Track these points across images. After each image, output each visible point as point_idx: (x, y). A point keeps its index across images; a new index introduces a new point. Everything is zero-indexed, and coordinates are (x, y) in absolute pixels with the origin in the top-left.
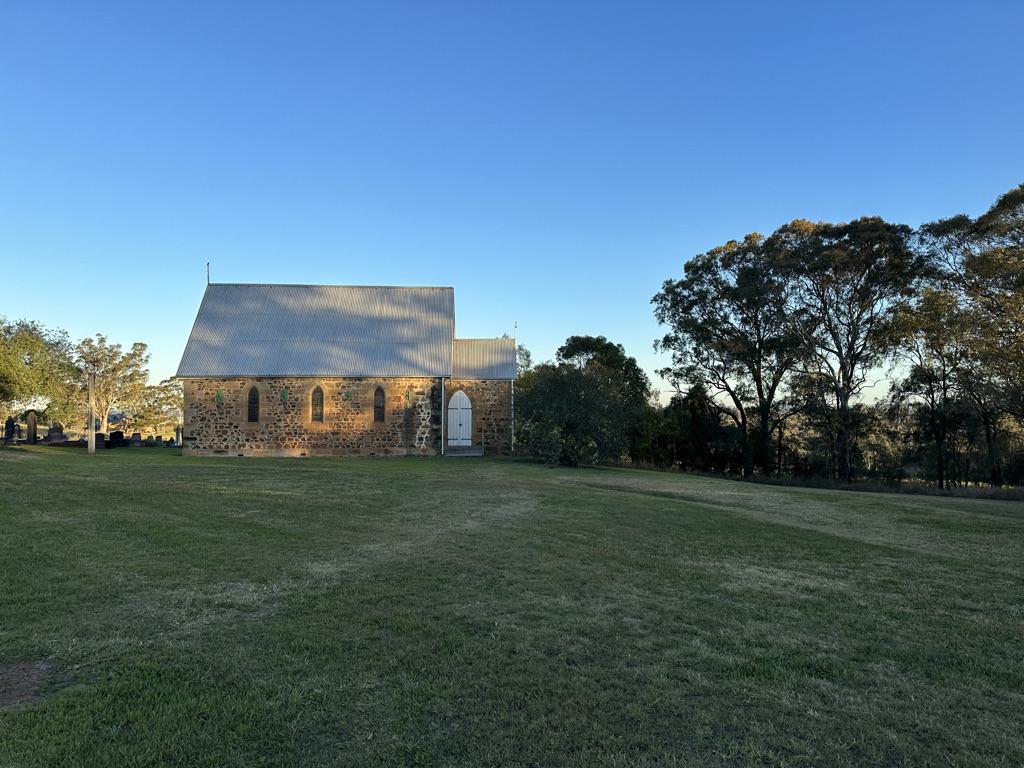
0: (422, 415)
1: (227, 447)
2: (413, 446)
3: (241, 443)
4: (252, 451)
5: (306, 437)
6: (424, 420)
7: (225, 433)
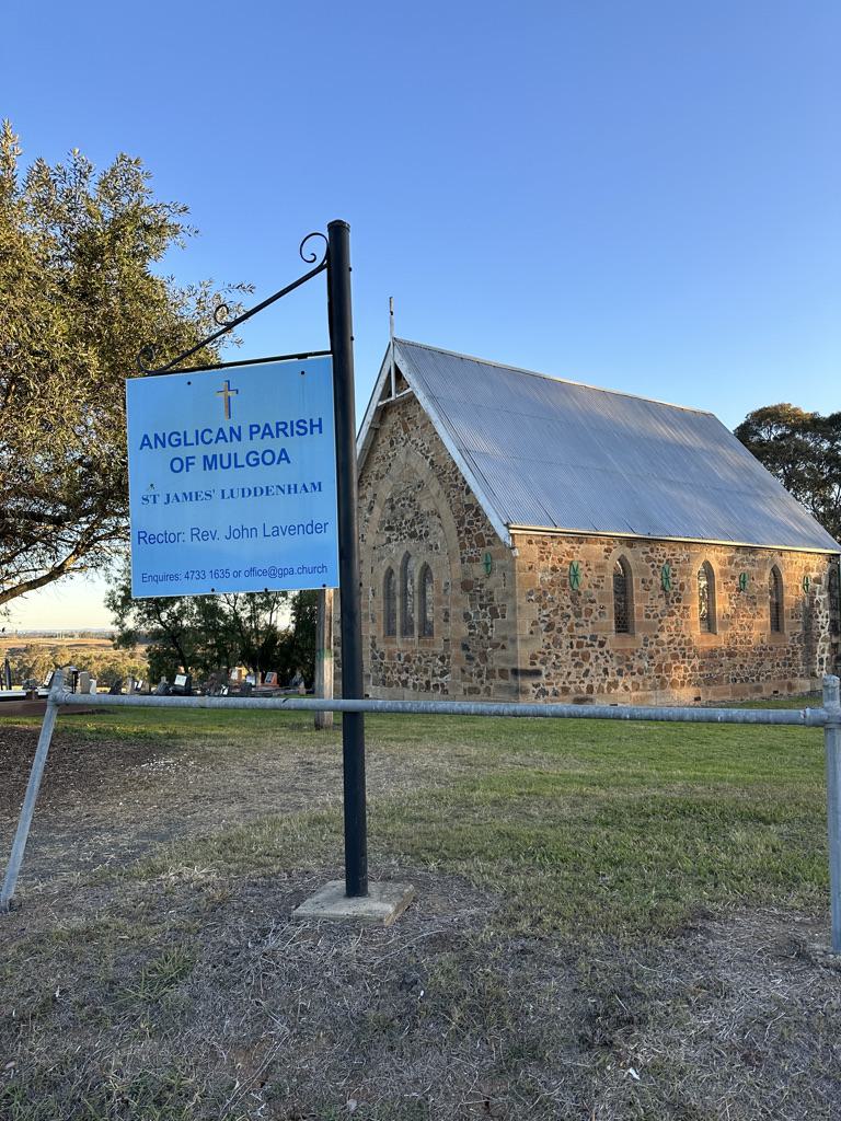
0: (820, 619)
1: (590, 689)
2: (814, 675)
3: (610, 679)
4: (625, 697)
5: (696, 662)
6: (823, 628)
7: (586, 657)
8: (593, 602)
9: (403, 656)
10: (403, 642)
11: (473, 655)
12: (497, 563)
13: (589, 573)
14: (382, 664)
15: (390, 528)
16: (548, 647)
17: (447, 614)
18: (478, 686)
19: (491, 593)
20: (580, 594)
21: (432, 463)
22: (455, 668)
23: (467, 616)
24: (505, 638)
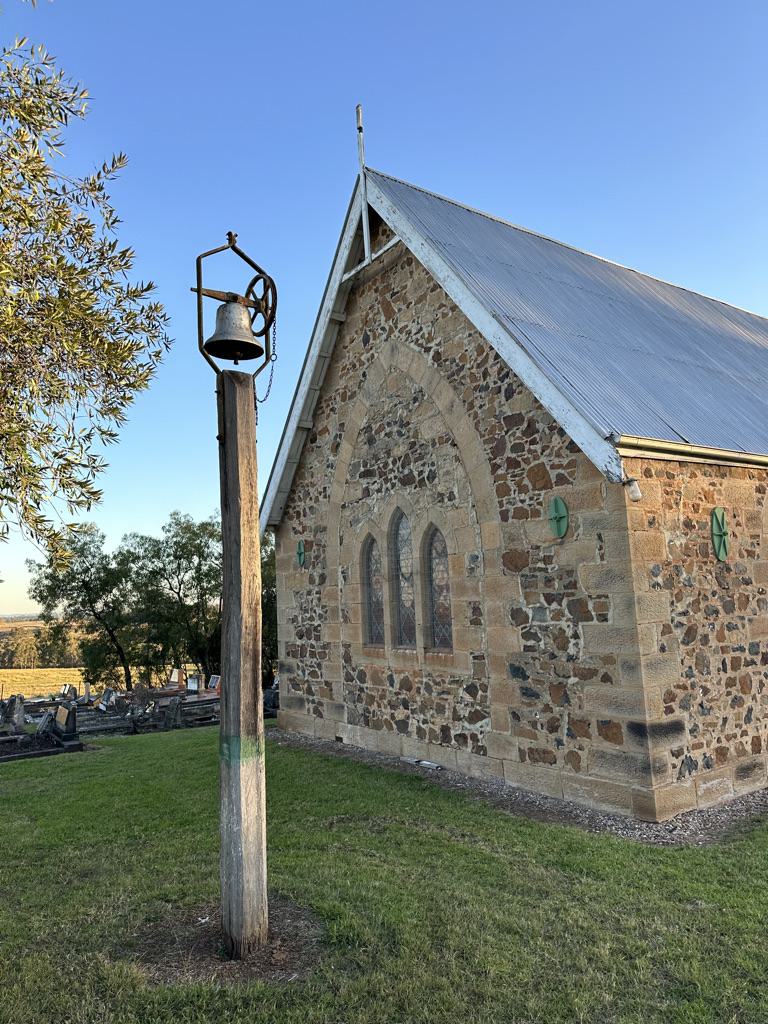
8: (748, 582)
9: (397, 679)
10: (396, 656)
11: (537, 688)
12: (581, 516)
13: (738, 530)
14: (361, 690)
15: (367, 474)
16: (689, 675)
17: (476, 610)
18: (551, 747)
19: (570, 573)
20: (729, 570)
21: (437, 357)
22: (499, 709)
23: (518, 616)
24: (608, 660)
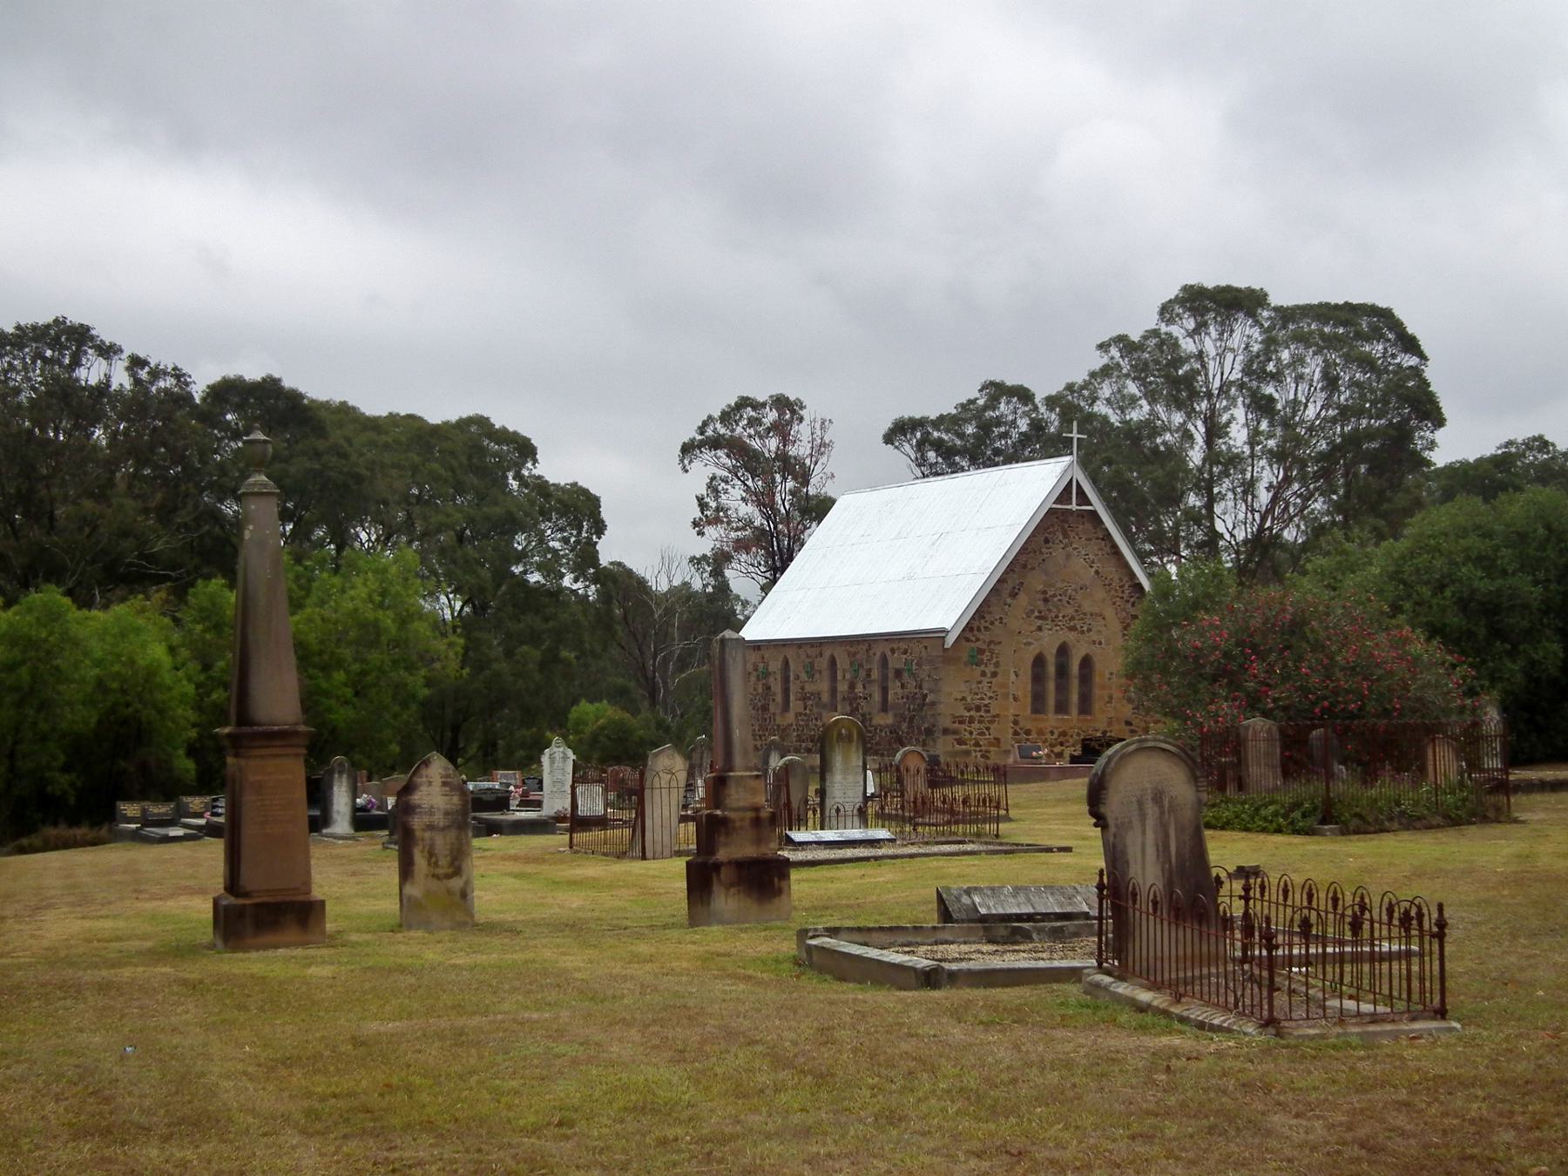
21: (1097, 572)
